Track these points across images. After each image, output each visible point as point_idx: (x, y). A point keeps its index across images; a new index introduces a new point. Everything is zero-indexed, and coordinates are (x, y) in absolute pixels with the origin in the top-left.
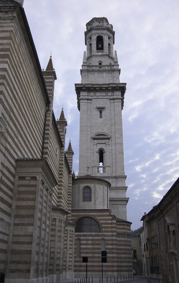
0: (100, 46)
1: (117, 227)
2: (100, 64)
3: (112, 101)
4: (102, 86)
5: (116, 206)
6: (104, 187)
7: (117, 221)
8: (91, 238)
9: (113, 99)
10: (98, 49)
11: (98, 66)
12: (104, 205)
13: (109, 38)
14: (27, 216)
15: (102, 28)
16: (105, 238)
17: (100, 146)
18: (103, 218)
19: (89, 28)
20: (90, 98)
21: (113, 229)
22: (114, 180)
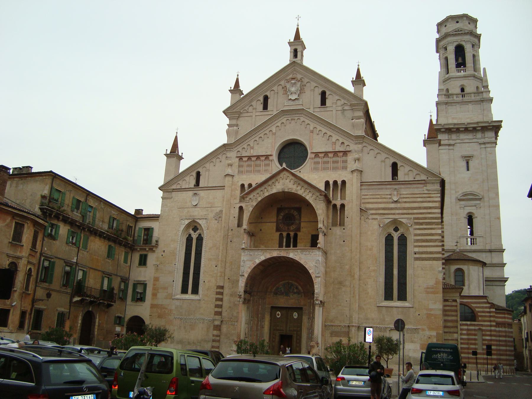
0: (460, 60)
1: (496, 315)
2: (463, 90)
3: (483, 146)
4: (467, 126)
5: (491, 287)
6: (479, 269)
7: (496, 309)
8: (466, 327)
9: (484, 143)
10: (458, 66)
11: (460, 94)
12: (479, 290)
13: (473, 46)
14: (453, 327)
15: (461, 33)
16: (481, 327)
17: (468, 210)
18: (478, 305)
19: (444, 30)
20: (452, 142)
21: (492, 319)
22: (488, 254)
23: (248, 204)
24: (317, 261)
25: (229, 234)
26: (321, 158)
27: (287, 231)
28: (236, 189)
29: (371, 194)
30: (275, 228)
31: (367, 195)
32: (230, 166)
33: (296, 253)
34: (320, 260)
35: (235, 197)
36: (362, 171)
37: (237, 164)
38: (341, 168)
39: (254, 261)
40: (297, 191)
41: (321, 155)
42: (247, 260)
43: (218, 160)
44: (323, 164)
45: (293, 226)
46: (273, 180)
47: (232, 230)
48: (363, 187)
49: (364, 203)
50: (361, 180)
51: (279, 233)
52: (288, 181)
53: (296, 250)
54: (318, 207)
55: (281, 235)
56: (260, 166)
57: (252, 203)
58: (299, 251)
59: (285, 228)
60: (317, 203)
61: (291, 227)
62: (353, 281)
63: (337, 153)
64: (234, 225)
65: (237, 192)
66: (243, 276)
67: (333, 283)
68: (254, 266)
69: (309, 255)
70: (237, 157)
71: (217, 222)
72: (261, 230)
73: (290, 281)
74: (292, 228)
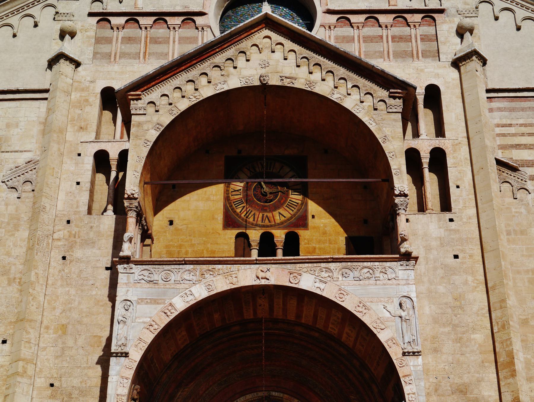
23: (142, 118)
24: (404, 299)
25: (56, 236)
26: (358, 27)
27: (263, 226)
28: (87, 101)
29: (521, 121)
30: (220, 217)
31: (510, 125)
32: (67, 37)
33: (324, 274)
34: (413, 295)
35: (83, 124)
36: (484, 61)
37: (92, 33)
38: (420, 55)
39: (167, 302)
40: (310, 83)
41: (354, 18)
42: (141, 301)
43: (30, 21)
44: (364, 41)
45: (281, 211)
46: (230, 52)
47: (68, 222)
48: (495, 104)
49: (503, 147)
50: (486, 85)
51: (236, 232)
52: (278, 55)
53: (323, 265)
54: (387, 131)
55: (243, 238)
56: (166, 41)
57: (156, 118)
58: (332, 266)
59: (254, 214)
60: (383, 120)
61: (276, 213)
62: (511, 380)
63: (405, 15)
64: (77, 207)
65: (88, 109)
66: (126, 355)
67: (436, 390)
68: (169, 320)
69: (372, 281)
70: (91, 14)
71: (16, 195)
72: (171, 223)
73: (274, 393)
74: (277, 217)
